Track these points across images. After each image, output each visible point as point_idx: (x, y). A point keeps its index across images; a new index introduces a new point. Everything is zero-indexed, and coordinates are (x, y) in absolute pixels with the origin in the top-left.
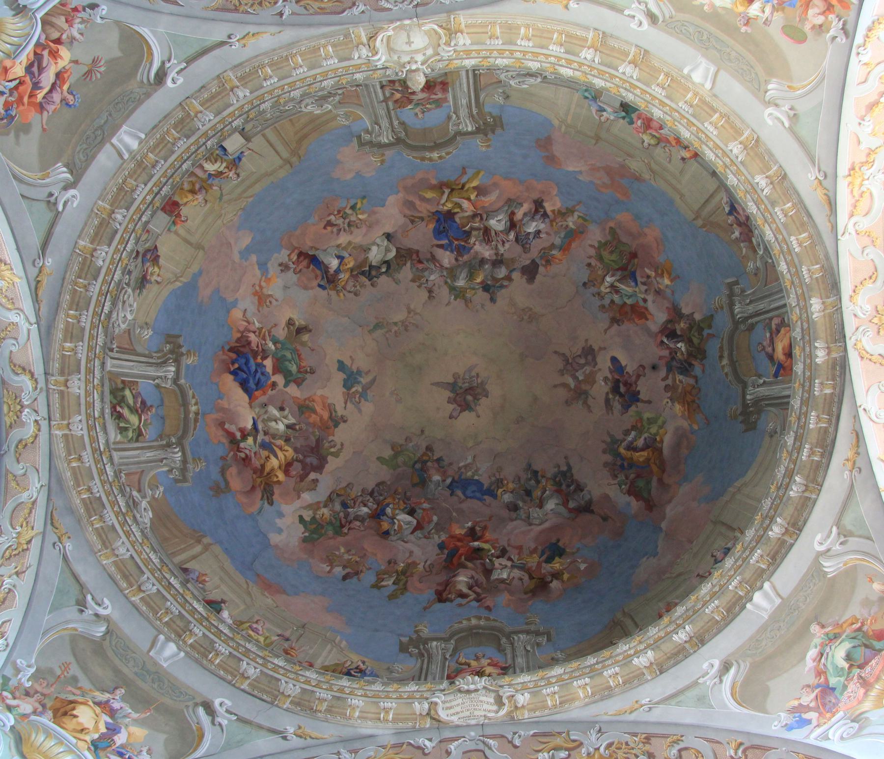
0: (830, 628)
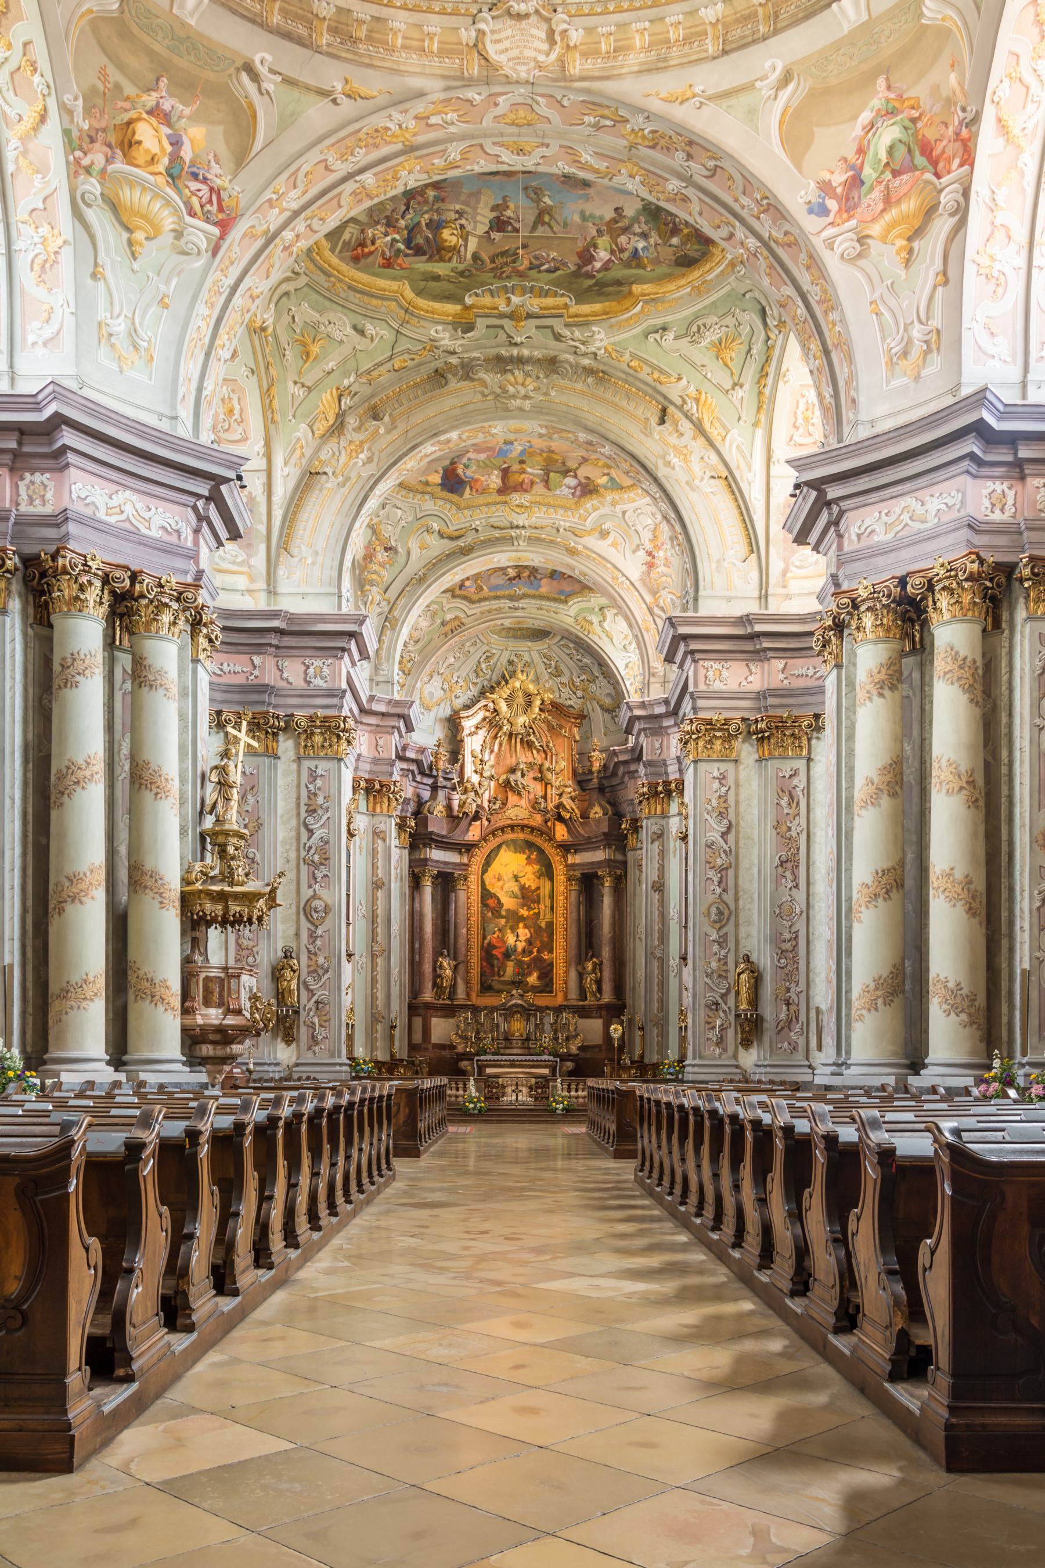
0: (892, 96)
